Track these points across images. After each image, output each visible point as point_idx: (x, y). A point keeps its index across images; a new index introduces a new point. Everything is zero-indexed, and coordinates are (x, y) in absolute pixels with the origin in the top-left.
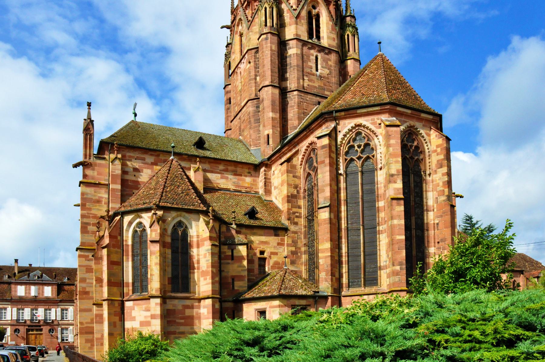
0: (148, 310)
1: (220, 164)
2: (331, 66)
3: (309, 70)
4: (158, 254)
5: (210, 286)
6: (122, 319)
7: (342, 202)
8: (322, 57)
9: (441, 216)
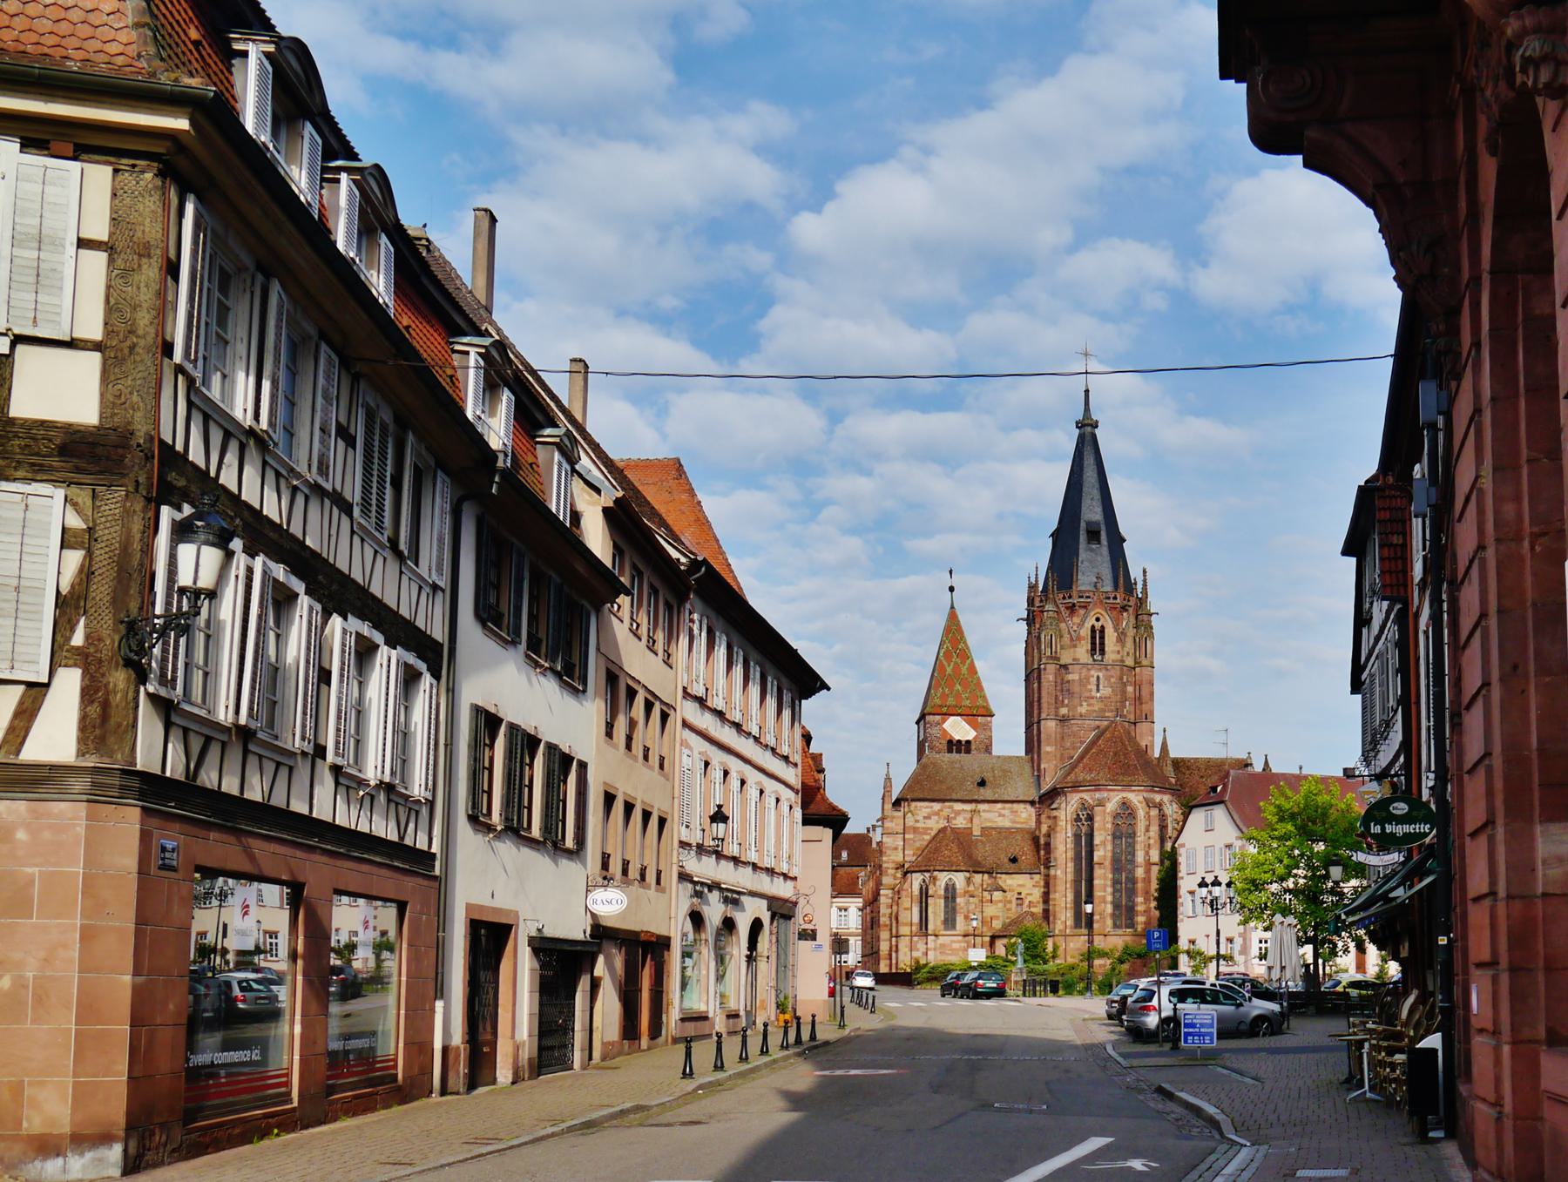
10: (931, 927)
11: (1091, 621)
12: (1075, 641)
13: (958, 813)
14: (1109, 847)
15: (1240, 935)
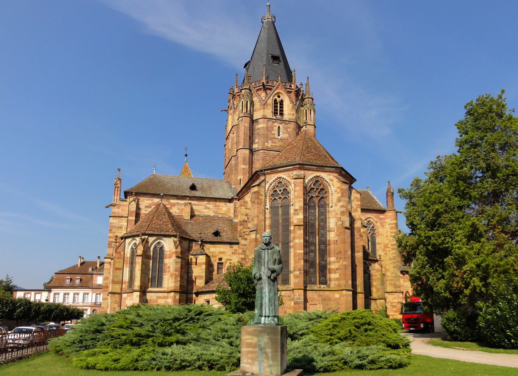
2: (290, 132)
3: (272, 136)
4: (141, 264)
5: (174, 283)
7: (267, 227)
9: (339, 235)
12: (265, 105)
13: (173, 205)
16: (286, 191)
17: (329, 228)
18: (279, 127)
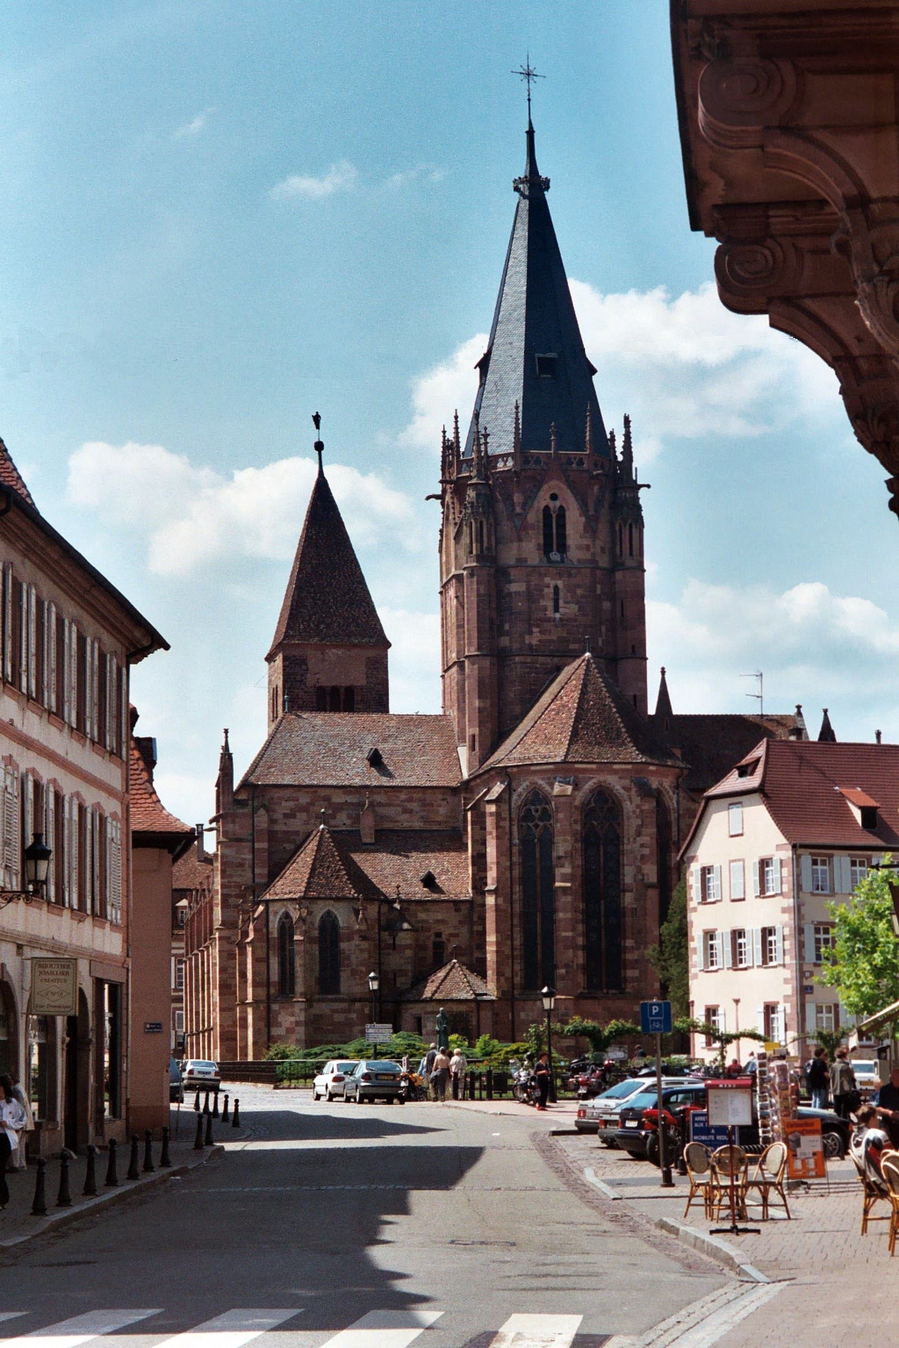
0: (293, 1015)
1: (401, 792)
2: (583, 596)
3: (541, 615)
6: (269, 1025)
8: (565, 586)
10: (299, 988)
11: (543, 500)
14: (579, 862)
15: (786, 998)
16: (546, 815)
17: (624, 884)
18: (556, 588)
